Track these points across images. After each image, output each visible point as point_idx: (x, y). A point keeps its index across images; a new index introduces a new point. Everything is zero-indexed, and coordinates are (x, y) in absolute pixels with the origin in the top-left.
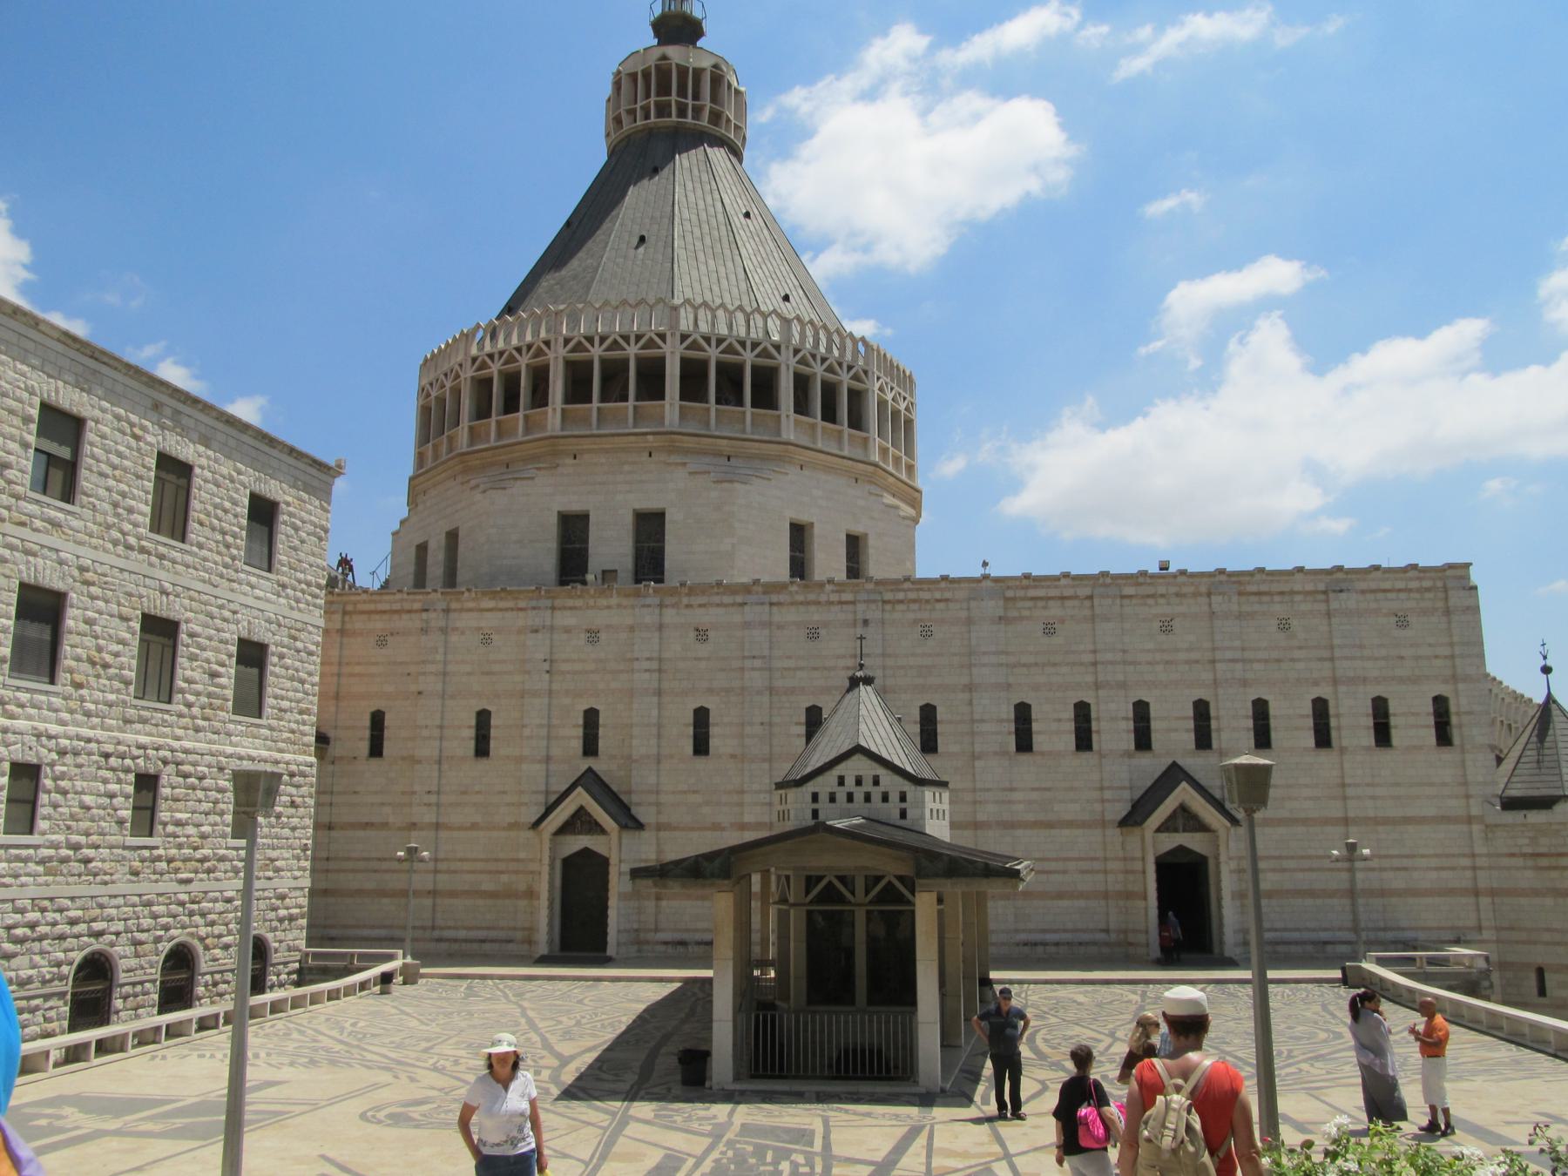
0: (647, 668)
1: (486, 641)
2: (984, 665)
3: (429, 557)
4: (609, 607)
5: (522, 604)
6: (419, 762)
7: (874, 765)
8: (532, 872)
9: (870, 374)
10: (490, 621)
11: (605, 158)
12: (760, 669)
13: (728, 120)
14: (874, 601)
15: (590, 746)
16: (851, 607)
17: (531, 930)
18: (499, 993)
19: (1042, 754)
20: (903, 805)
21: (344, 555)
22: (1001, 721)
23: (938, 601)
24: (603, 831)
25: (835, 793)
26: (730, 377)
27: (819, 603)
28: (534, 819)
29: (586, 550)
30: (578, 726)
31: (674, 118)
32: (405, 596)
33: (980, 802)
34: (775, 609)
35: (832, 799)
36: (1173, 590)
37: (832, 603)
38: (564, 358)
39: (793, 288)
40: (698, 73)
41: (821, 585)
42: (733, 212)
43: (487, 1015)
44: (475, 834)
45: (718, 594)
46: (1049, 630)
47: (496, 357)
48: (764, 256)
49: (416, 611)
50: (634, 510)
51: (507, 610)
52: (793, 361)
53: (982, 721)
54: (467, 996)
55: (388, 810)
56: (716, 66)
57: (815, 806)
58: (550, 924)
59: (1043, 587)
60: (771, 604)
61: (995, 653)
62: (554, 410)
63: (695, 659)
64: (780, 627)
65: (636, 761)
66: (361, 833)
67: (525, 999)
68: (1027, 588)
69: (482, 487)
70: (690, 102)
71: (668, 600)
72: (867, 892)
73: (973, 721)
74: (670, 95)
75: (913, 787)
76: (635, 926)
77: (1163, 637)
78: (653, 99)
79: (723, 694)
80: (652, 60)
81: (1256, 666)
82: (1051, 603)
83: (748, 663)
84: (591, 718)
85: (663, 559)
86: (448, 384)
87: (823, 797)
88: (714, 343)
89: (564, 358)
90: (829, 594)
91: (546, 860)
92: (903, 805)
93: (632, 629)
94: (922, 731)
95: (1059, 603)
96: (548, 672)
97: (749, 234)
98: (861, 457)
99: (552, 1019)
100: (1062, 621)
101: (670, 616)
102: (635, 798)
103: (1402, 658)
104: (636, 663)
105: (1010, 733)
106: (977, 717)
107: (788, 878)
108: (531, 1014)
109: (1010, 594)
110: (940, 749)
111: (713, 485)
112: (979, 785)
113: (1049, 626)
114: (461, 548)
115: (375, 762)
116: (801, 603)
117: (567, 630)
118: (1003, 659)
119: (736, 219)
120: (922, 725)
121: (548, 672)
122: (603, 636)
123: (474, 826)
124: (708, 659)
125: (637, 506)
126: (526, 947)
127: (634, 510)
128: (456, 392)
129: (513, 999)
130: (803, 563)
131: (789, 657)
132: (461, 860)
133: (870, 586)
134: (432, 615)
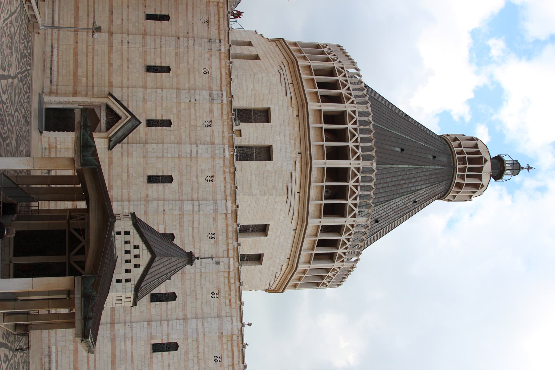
0: (192, 151)
1: (205, 71)
2: (197, 325)
3: (246, 47)
4: (223, 132)
5: (224, 88)
6: (144, 38)
7: (145, 265)
8: (87, 94)
9: (342, 264)
10: (215, 72)
11: (438, 133)
12: (193, 210)
13: (458, 192)
14: (229, 267)
15: (151, 123)
16: (225, 255)
17: (57, 94)
18: (23, 70)
19: (151, 358)
20: (124, 281)
21: (242, 14)
22: (168, 336)
23: (230, 301)
24: (107, 129)
25: (130, 243)
26: (341, 193)
27: (228, 239)
28: (114, 94)
29: (251, 122)
30: (162, 117)
31: (458, 166)
32: (227, 32)
33: (125, 325)
34: (224, 216)
35: (127, 242)
37: (228, 245)
38: (346, 110)
39: (381, 224)
40: (480, 177)
41: (237, 240)
42: (416, 195)
43: (10, 57)
44: (107, 65)
45: (231, 187)
46: (217, 359)
47: (345, 78)
48: (396, 210)
49: (219, 37)
50: (272, 145)
51: (221, 81)
52: (347, 224)
53: (168, 325)
54: (22, 53)
55: (119, 22)
56: (483, 186)
57: (123, 233)
58: (60, 103)
59: (239, 355)
60: (226, 215)
61: (204, 331)
62: (321, 106)
63: (197, 176)
64: (215, 219)
65: (144, 146)
66: (107, 9)
67: (19, 81)
68: (238, 347)
69: (281, 71)
70: (466, 173)
71: (227, 162)
72: (76, 262)
73: (168, 320)
74: (468, 164)
75: (133, 286)
76: (59, 147)
78: (467, 156)
79: (180, 190)
80: (484, 155)
82: (230, 359)
83: (196, 203)
84: (168, 123)
85: (247, 160)
86: (330, 56)
87: (127, 238)
88: (356, 184)
89: (346, 110)
90: (232, 243)
91: (93, 100)
92: (124, 281)
93: (212, 144)
94: (162, 294)
95: (231, 364)
96: (190, 101)
97: (406, 202)
98: (301, 260)
99: (6, 89)
100: (221, 366)
101: (219, 163)
102: (125, 146)
104: (195, 146)
105: (162, 340)
106: (170, 322)
107: (84, 219)
108: (10, 80)
109: (235, 338)
110: (152, 303)
111: (285, 185)
112: (134, 324)
113: (218, 359)
114: (250, 61)
115: (144, 16)
116: (227, 230)
117: (211, 111)
118: (201, 336)
119: (413, 196)
120: (165, 293)
121: (190, 101)
122: (209, 129)
123: (110, 65)
124: (198, 182)
125: (273, 147)
126: (48, 91)
127: (272, 145)
128: (328, 60)
129: (19, 76)
130: (246, 232)
131: (199, 224)
132: (93, 58)
133: (237, 265)
134: (218, 45)
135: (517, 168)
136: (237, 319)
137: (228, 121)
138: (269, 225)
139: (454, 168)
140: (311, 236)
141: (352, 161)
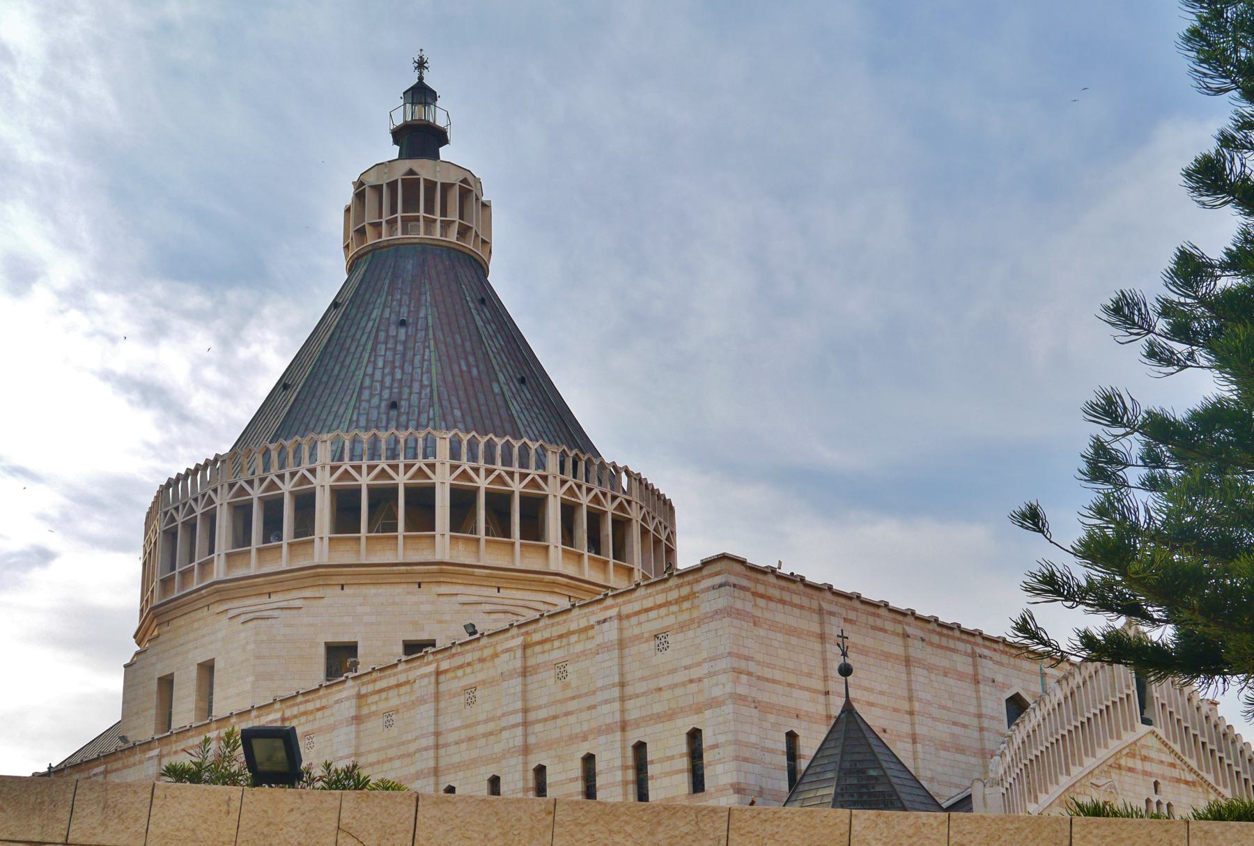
4: (134, 764)
23: (318, 710)
36: (477, 655)
45: (192, 736)
56: (411, 172)
68: (375, 681)
88: (256, 483)
95: (396, 690)
98: (430, 558)
100: (397, 712)
103: (660, 689)
109: (364, 690)
111: (242, 627)
125: (200, 662)
135: (421, 94)
136: (340, 691)
137: (124, 756)
138: (325, 643)
139: (375, 248)
140: (358, 552)
141: (217, 501)
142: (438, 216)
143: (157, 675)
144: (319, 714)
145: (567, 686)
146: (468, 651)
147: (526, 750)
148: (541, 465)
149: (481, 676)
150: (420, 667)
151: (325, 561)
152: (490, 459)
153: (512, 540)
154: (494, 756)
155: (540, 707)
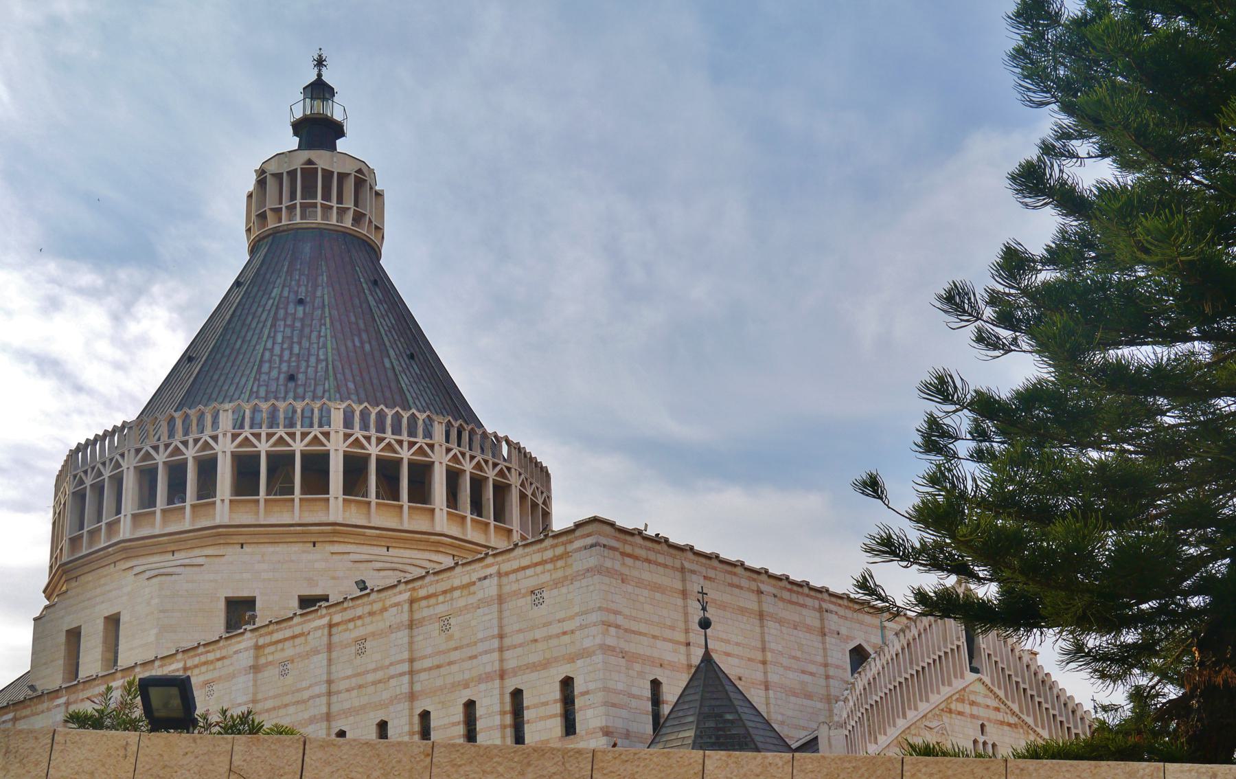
4: (43, 712)
23: (218, 660)
36: (367, 609)
45: (98, 685)
56: (310, 162)
68: (272, 633)
77: (358, 660)
81: (423, 676)
88: (162, 448)
95: (291, 642)
98: (324, 519)
100: (293, 661)
103: (536, 641)
109: (261, 642)
111: (147, 583)
125: (107, 615)
135: (319, 90)
136: (239, 642)
137: (32, 704)
138: (226, 598)
139: (275, 232)
140: (257, 513)
141: (124, 465)
142: (334, 203)
143: (66, 628)
144: (219, 664)
145: (451, 638)
146: (358, 606)
147: (412, 697)
148: (427, 434)
149: (370, 629)
150: (314, 620)
151: (226, 521)
152: (381, 428)
153: (400, 503)
154: (382, 703)
155: (424, 657)
